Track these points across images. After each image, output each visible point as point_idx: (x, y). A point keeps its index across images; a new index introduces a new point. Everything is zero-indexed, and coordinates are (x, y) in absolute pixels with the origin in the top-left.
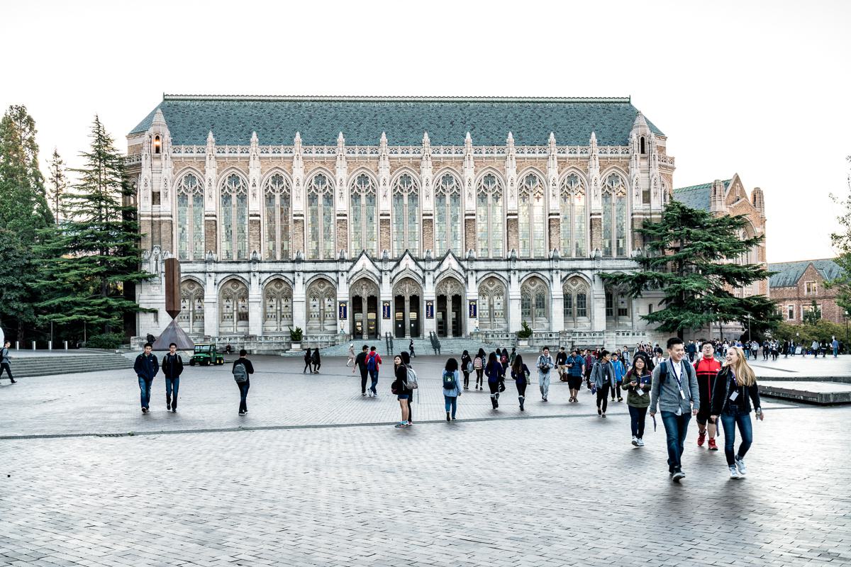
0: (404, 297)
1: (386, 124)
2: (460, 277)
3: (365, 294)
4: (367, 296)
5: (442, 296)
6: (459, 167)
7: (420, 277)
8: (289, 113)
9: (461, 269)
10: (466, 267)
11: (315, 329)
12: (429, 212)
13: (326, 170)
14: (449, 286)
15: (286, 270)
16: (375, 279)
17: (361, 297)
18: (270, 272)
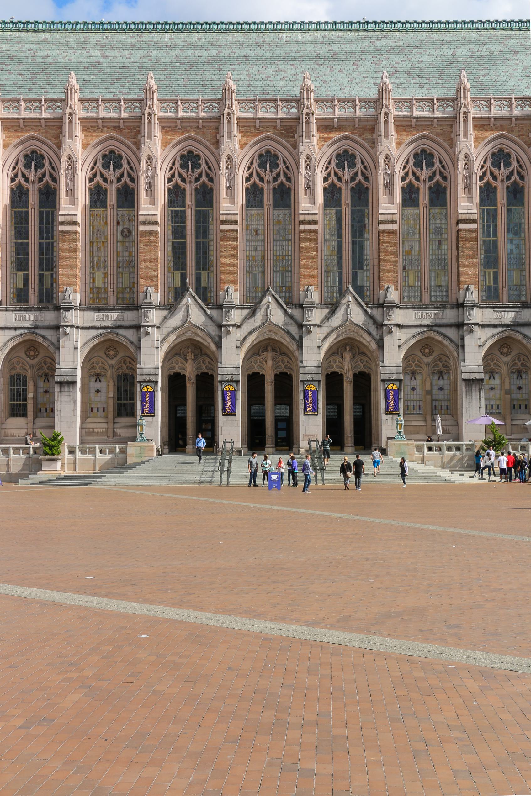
0: (263, 376)
1: (237, 67)
2: (368, 338)
3: (190, 370)
4: (196, 373)
5: (335, 374)
6: (368, 135)
7: (293, 338)
8: (66, 48)
9: (370, 322)
10: (379, 318)
11: (98, 434)
12: (310, 218)
13: (122, 142)
14: (348, 356)
15: (45, 323)
16: (209, 340)
17: (184, 376)
18: (16, 329)
